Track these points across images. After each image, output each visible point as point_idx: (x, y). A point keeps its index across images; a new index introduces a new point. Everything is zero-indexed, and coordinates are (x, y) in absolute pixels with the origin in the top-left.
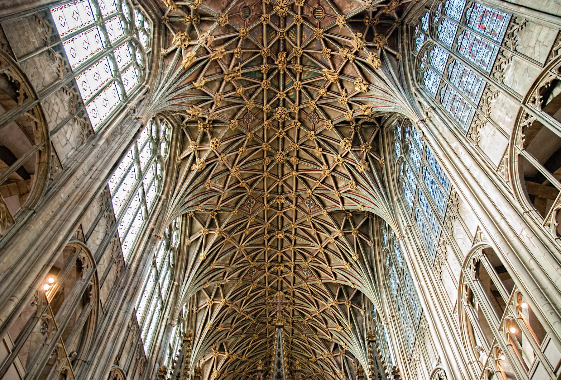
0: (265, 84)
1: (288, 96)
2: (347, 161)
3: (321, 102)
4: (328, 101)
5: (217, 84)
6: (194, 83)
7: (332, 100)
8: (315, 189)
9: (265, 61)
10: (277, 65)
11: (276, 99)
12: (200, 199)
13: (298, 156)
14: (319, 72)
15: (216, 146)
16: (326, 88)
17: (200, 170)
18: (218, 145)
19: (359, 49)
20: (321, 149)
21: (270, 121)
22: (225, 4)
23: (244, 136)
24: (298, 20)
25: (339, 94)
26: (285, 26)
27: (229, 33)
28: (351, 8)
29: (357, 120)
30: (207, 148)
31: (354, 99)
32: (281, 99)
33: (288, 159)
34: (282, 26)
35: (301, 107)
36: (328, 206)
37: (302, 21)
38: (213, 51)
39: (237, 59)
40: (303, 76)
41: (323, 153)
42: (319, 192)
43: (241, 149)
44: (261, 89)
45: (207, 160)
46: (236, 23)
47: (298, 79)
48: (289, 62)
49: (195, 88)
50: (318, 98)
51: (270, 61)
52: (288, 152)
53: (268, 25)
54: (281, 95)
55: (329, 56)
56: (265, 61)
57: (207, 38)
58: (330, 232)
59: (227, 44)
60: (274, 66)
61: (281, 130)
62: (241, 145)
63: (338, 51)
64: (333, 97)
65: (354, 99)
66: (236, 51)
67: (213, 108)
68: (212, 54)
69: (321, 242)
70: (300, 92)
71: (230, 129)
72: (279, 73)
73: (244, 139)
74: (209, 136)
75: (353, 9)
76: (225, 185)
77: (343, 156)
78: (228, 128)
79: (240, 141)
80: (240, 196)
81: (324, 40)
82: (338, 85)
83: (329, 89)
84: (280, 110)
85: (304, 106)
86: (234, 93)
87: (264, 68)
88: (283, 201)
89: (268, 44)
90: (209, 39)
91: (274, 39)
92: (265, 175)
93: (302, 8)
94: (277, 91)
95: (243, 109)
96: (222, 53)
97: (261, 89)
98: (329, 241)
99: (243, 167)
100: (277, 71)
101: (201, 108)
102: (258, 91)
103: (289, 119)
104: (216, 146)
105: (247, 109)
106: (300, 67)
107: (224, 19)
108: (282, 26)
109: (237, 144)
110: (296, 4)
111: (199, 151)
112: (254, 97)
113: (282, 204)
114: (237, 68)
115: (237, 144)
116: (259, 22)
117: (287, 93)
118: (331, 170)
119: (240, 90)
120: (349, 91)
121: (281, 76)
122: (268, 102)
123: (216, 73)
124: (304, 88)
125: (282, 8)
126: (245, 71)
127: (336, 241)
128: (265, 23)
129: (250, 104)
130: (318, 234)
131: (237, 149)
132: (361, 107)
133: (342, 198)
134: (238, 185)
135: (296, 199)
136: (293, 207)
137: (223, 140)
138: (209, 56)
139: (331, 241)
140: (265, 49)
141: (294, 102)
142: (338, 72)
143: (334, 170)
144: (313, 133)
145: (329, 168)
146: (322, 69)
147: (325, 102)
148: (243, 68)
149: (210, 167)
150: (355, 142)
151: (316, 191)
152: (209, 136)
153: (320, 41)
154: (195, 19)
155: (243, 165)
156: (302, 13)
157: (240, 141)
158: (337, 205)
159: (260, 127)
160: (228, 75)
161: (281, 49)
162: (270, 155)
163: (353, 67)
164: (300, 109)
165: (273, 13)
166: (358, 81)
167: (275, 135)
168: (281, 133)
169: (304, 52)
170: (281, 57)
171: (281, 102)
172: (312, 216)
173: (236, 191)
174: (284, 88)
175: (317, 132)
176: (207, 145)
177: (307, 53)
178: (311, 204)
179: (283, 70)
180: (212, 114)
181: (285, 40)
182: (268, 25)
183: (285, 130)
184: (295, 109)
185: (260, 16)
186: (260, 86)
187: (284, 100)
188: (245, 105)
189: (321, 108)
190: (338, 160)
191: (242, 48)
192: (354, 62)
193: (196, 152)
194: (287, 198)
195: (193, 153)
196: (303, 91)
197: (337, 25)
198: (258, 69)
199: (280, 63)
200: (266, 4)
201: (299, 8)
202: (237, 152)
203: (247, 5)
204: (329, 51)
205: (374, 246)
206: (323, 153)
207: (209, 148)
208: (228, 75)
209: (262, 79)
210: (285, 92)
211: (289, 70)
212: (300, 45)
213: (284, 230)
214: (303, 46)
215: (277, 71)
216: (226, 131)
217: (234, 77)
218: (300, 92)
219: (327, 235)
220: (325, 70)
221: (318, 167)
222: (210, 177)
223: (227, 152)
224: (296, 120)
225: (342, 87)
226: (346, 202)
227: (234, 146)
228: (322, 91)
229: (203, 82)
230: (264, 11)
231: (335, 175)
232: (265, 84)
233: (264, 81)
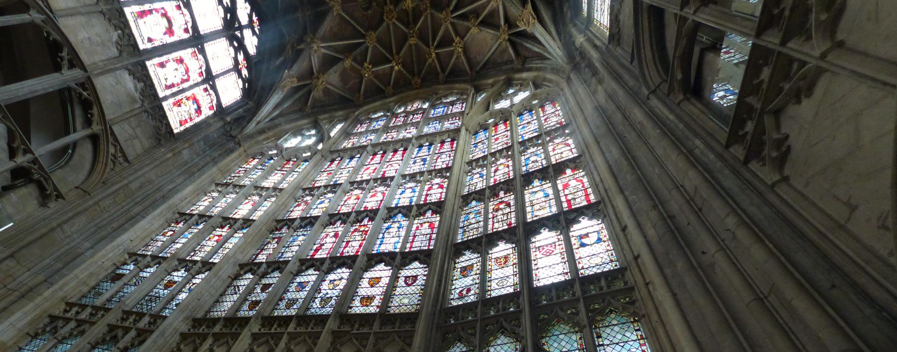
28: (331, 27)
75: (329, 28)
110: (392, 7)
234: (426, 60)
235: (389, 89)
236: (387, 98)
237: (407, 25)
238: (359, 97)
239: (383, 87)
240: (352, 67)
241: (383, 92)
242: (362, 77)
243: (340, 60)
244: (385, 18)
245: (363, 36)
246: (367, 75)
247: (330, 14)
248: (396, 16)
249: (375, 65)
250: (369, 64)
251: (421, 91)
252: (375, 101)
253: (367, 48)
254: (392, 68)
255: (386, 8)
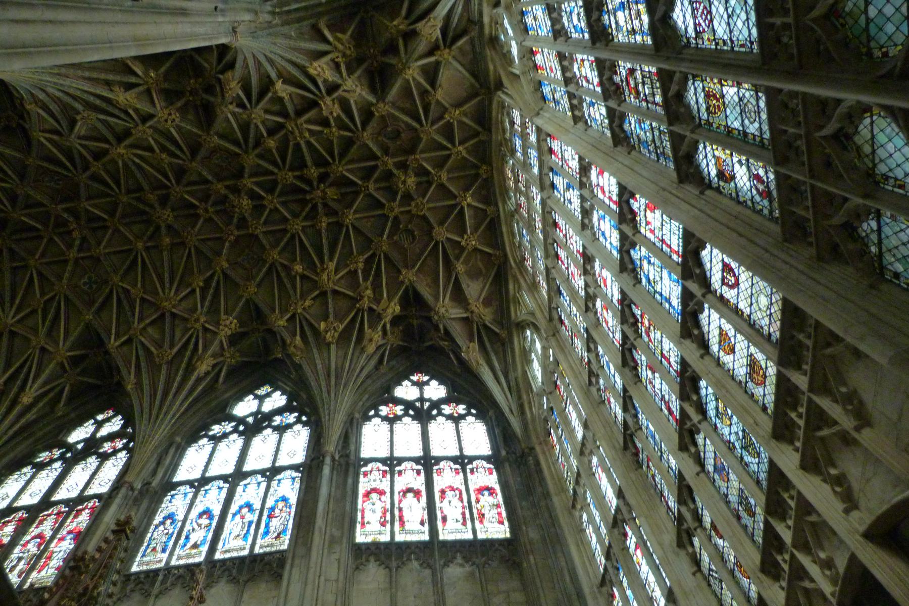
0: (289, 177)
1: (271, 210)
2: (201, 335)
3: (280, 269)
4: (286, 280)
5: (276, 108)
6: (280, 81)
7: (289, 286)
8: (123, 288)
9: (322, 170)
10: (318, 188)
11: (263, 194)
12: (53, 107)
13: (173, 245)
14: (326, 257)
15: (166, 121)
16: (305, 272)
17: (115, 102)
18: (169, 122)
19: (379, 314)
20: (201, 284)
21: (223, 191)
22: (402, 105)
23: (190, 157)
24: (392, 209)
25: (303, 297)
26: (377, 189)
27: (360, 116)
29: (271, 332)
30: (158, 105)
31: (304, 323)
32: (265, 203)
33: (163, 231)
34: (378, 185)
35: (261, 236)
36: (100, 317)
37: (392, 215)
38: (333, 100)
39: (322, 132)
40: (309, 231)
41: (198, 290)
42: (122, 296)
43: (164, 156)
44: (276, 170)
45: (136, 110)
46: (373, 125)
47: (304, 224)
48: (325, 205)
49: (271, 83)
50: (286, 263)
51: (323, 178)
52: (176, 226)
53: (375, 167)
54: (272, 201)
55: (352, 267)
56: (322, 170)
57: (354, 91)
58: (51, 334)
59: (343, 117)
60: (315, 183)
61: (211, 210)
62: (172, 155)
63: (366, 279)
64: (294, 288)
65: (304, 323)
66: (334, 129)
67: (237, 110)
68: (328, 100)
69: (19, 321)
70: (285, 231)
71: (200, 136)
72: (304, 192)
73: (184, 157)
74: (179, 104)
76: (85, 138)
77: (207, 325)
78: (200, 133)
79: (178, 152)
80: (68, 164)
81: (374, 255)
82: (317, 293)
83: (303, 277)
84: (246, 202)
85: (264, 242)
86: (265, 135)
87: (313, 172)
88: (76, 234)
89: (348, 170)
90: (352, 94)
91: (356, 177)
92: (124, 199)
93: (409, 212)
94: (276, 194)
95: (237, 150)
96: (331, 113)
97: (276, 170)
98: (32, 338)
99: (130, 164)
100: (307, 188)
101: (238, 95)
102: (271, 168)
103: (235, 220)
104: (166, 121)
105: (238, 155)
106: (324, 225)
107: (383, 109)
108: (378, 185)
109: (173, 148)
111: (148, 91)
112: (261, 162)
113: (70, 233)
114: (307, 135)
115: (173, 148)
116: (379, 154)
117: (276, 209)
118: (174, 310)
119: (272, 143)
120: (312, 311)
121: (301, 197)
122: (256, 184)
123: (295, 105)
124: (293, 237)
125: (404, 182)
126: (305, 150)
127: (38, 351)
128: (379, 163)
129: (251, 160)
130: (34, 311)
131: (163, 149)
132: (298, 338)
133: (129, 341)
134: (91, 159)
135: (91, 257)
136: (73, 254)
137: (179, 129)
138: (325, 95)
139: (34, 343)
140: (340, 169)
141: (265, 223)
142: (337, 288)
143: (174, 315)
144: (225, 265)
145: (174, 307)
146: (331, 259)
147: (283, 274)
148: (308, 143)
149: (122, 115)
150: (234, 340)
151: (120, 290)
152: (179, 104)
153: (371, 249)
154: (375, 64)
155: (134, 162)
156: (402, 213)
157: (178, 152)
158: (113, 337)
159: (210, 178)
160: (296, 125)
161: (343, 191)
162: (164, 201)
163: (350, 311)
164: (257, 236)
165: (395, 171)
166: (335, 325)
167: (200, 201)
168: (206, 211)
169: (347, 227)
170: (331, 193)
171: (258, 203)
172: (68, 293)
173: (76, 156)
174: (284, 204)
175: (228, 272)
176: (163, 104)
177: (348, 230)
178: (91, 287)
179: (312, 199)
180: (228, 113)
181: (357, 193)
182: (375, 167)
183: (213, 216)
184: (256, 228)
185: (387, 155)
186: (279, 169)
187: (264, 207)
188: (246, 152)
189: (270, 268)
190: (197, 320)
191: (341, 137)
192: (359, 310)
193: (145, 87)
194: (84, 239)
195: (141, 82)
196: (288, 235)
197: (399, 272)
198: (309, 163)
199: (323, 191)
200: (407, 160)
201: (408, 208)
202: (158, 151)
203: (403, 135)
204: (361, 265)
205: (59, 418)
206: (198, 290)
207: (159, 108)
208: (296, 125)
209: (291, 169)
210: (278, 206)
211: (315, 207)
212: (356, 219)
213: (13, 246)
214: (356, 224)
215: (307, 188)
216: (195, 130)
217: (292, 133)
218: (285, 231)
219: (42, 331)
220: (332, 266)
221: (167, 285)
222: (102, 117)
223: (156, 136)
224: (236, 233)
225: (313, 299)
226: (125, 348)
227: (168, 145)
228: (298, 268)
229: (283, 95)
230: (396, 160)
231: (168, 319)
232: (289, 177)
233: (290, 174)
234: (464, 158)
235: (490, 210)
236: (499, 215)
237: (430, 184)
238: (495, 255)
239: (488, 220)
240: (466, 262)
241: (492, 220)
242: (476, 250)
243: (457, 279)
244: (422, 213)
245: (437, 243)
246: (474, 243)
247: (415, 285)
248: (421, 199)
249: (465, 232)
250: (463, 238)
251: (494, 165)
252: (502, 233)
253: (448, 239)
254: (469, 205)
255: (414, 211)
